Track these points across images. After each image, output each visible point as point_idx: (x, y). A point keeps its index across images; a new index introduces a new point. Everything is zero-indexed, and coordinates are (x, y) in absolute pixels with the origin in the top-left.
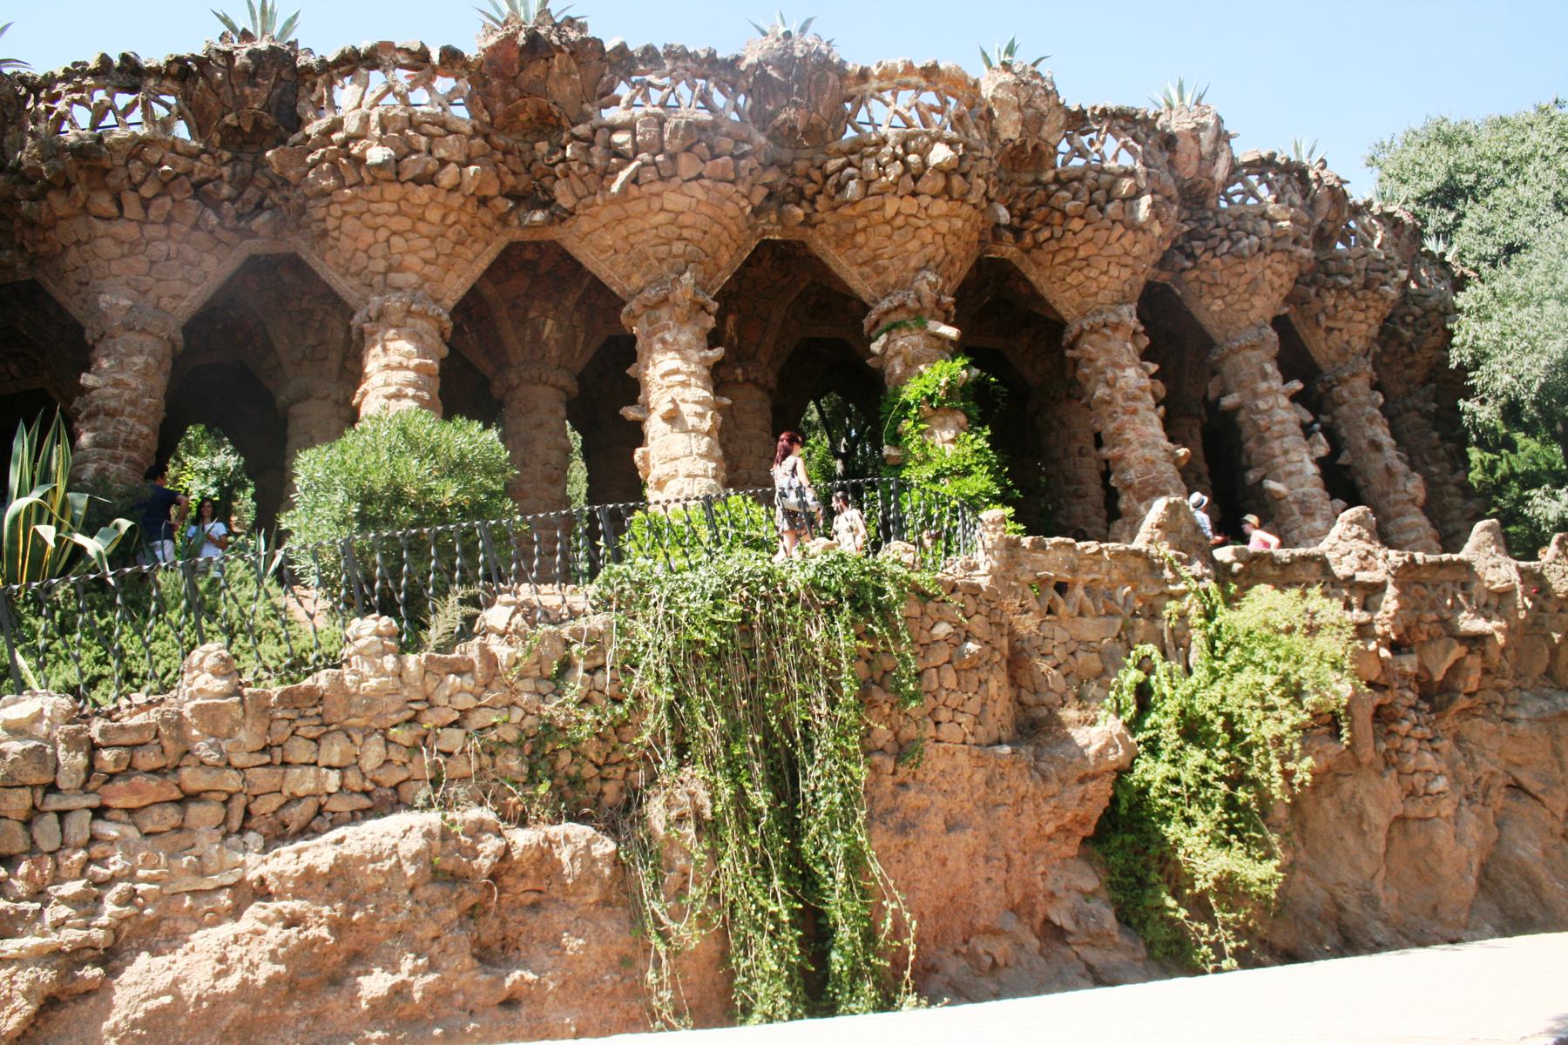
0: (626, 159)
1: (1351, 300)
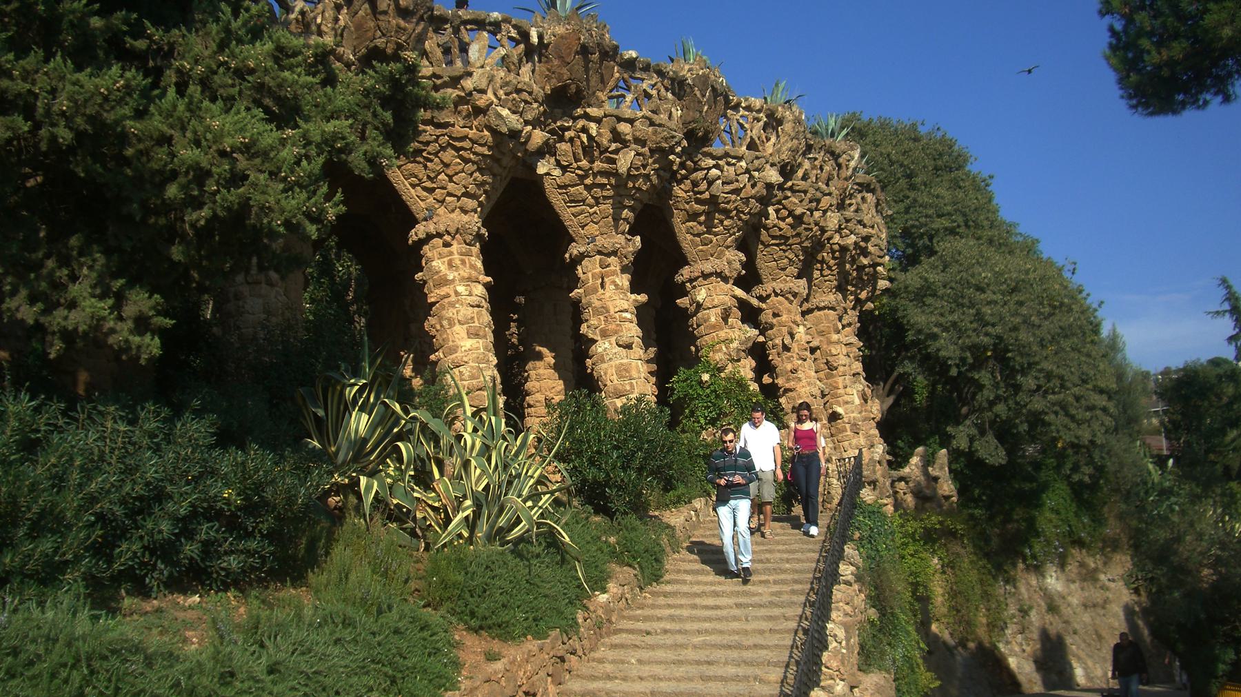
0: (625, 144)
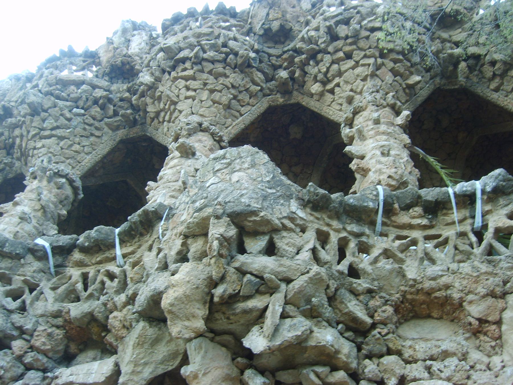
1: (328, 58)
